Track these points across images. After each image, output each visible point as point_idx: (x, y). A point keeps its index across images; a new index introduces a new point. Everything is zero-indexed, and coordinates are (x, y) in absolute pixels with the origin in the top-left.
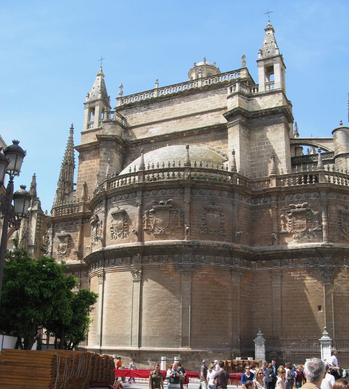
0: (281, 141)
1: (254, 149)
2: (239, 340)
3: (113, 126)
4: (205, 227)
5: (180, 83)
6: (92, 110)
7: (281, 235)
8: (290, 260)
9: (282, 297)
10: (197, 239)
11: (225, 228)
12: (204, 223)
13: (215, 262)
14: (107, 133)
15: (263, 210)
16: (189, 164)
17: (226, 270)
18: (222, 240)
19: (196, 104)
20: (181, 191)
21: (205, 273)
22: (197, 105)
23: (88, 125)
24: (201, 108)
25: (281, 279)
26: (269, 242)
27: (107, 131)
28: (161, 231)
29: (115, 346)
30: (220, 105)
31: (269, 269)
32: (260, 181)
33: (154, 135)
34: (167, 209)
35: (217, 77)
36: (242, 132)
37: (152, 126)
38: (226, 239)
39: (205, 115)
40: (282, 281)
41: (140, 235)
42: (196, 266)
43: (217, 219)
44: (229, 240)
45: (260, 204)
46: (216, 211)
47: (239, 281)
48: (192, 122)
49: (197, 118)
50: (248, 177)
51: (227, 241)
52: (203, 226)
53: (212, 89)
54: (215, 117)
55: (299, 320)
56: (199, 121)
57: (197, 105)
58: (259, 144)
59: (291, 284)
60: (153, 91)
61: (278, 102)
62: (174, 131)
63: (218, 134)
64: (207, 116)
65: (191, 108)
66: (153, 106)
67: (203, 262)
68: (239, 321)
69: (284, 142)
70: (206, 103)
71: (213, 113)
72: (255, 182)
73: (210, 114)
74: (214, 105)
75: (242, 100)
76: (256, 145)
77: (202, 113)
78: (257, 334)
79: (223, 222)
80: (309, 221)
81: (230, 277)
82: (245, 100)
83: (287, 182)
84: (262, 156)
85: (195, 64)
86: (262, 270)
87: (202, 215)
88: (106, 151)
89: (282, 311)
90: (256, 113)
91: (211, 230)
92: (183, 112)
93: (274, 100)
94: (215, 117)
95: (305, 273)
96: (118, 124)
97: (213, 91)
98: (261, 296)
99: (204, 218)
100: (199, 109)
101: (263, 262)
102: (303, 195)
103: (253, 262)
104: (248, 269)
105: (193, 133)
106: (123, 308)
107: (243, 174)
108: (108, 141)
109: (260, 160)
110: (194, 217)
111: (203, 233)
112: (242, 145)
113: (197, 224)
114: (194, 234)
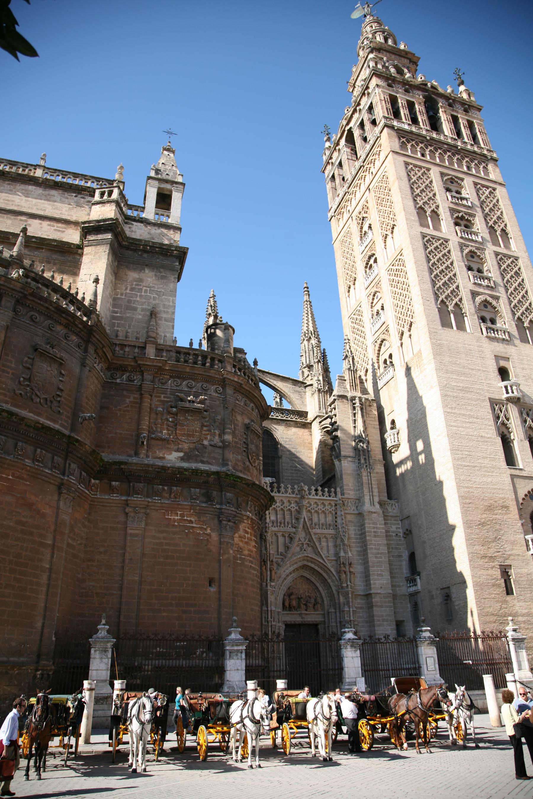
4: (28, 386)
7: (153, 442)
8: (166, 488)
9: (143, 555)
10: (7, 402)
12: (28, 377)
13: (34, 460)
15: (125, 393)
24: (32, 208)
30: (69, 215)
36: (110, 259)
40: (146, 524)
51: (62, 425)
52: (24, 382)
53: (59, 189)
54: (55, 230)
55: (173, 602)
58: (132, 289)
59: (162, 532)
63: (55, 256)
64: (41, 224)
65: (13, 201)
67: (9, 455)
80: (205, 428)
81: (56, 497)
84: (135, 309)
89: (141, 583)
90: (137, 243)
94: (55, 230)
95: (191, 515)
97: (61, 192)
98: (102, 550)
99: (30, 366)
101: (114, 483)
102: (199, 385)
105: (9, 239)
109: (129, 313)
110: (9, 358)
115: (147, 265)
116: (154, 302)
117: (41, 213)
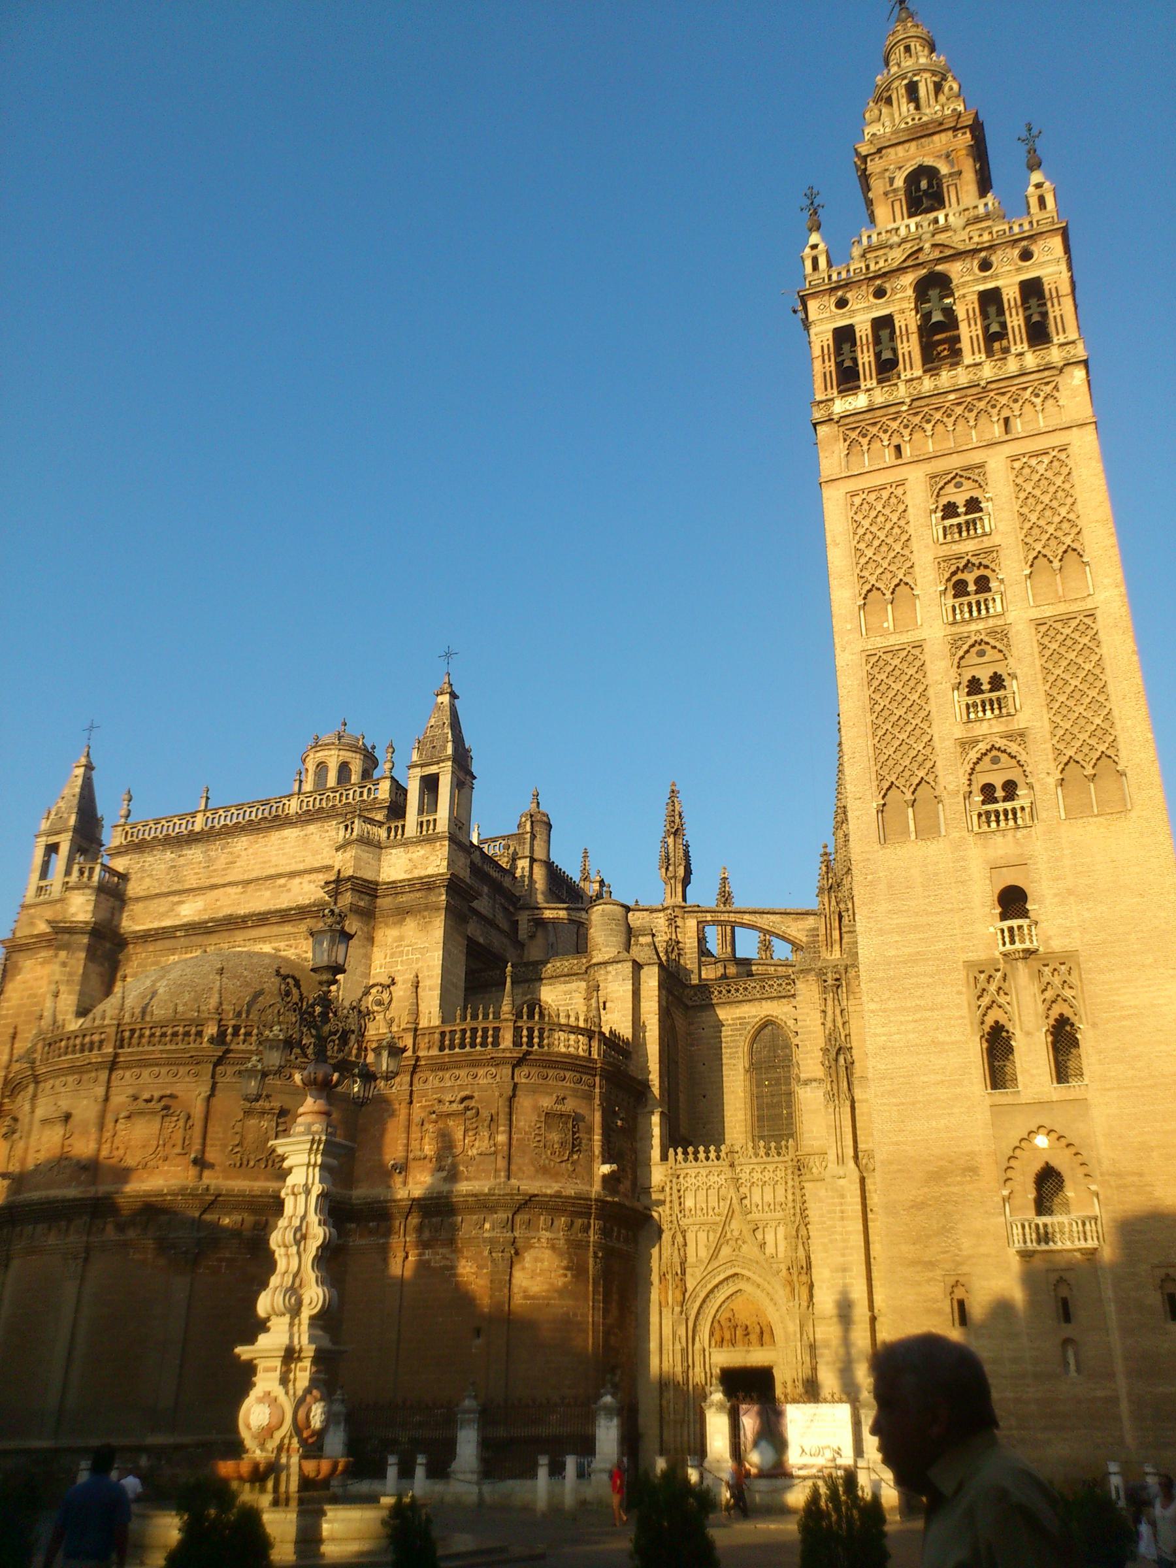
6: (52, 849)
19: (281, 852)
22: (283, 854)
23: (40, 889)
33: (185, 920)
39: (297, 880)
48: (268, 894)
49: (280, 886)
56: (282, 892)
57: (283, 854)
62: (229, 913)
65: (270, 861)
69: (441, 952)
71: (314, 876)
73: (307, 877)
77: (292, 875)
92: (253, 870)
93: (432, 858)
117: (301, 867)
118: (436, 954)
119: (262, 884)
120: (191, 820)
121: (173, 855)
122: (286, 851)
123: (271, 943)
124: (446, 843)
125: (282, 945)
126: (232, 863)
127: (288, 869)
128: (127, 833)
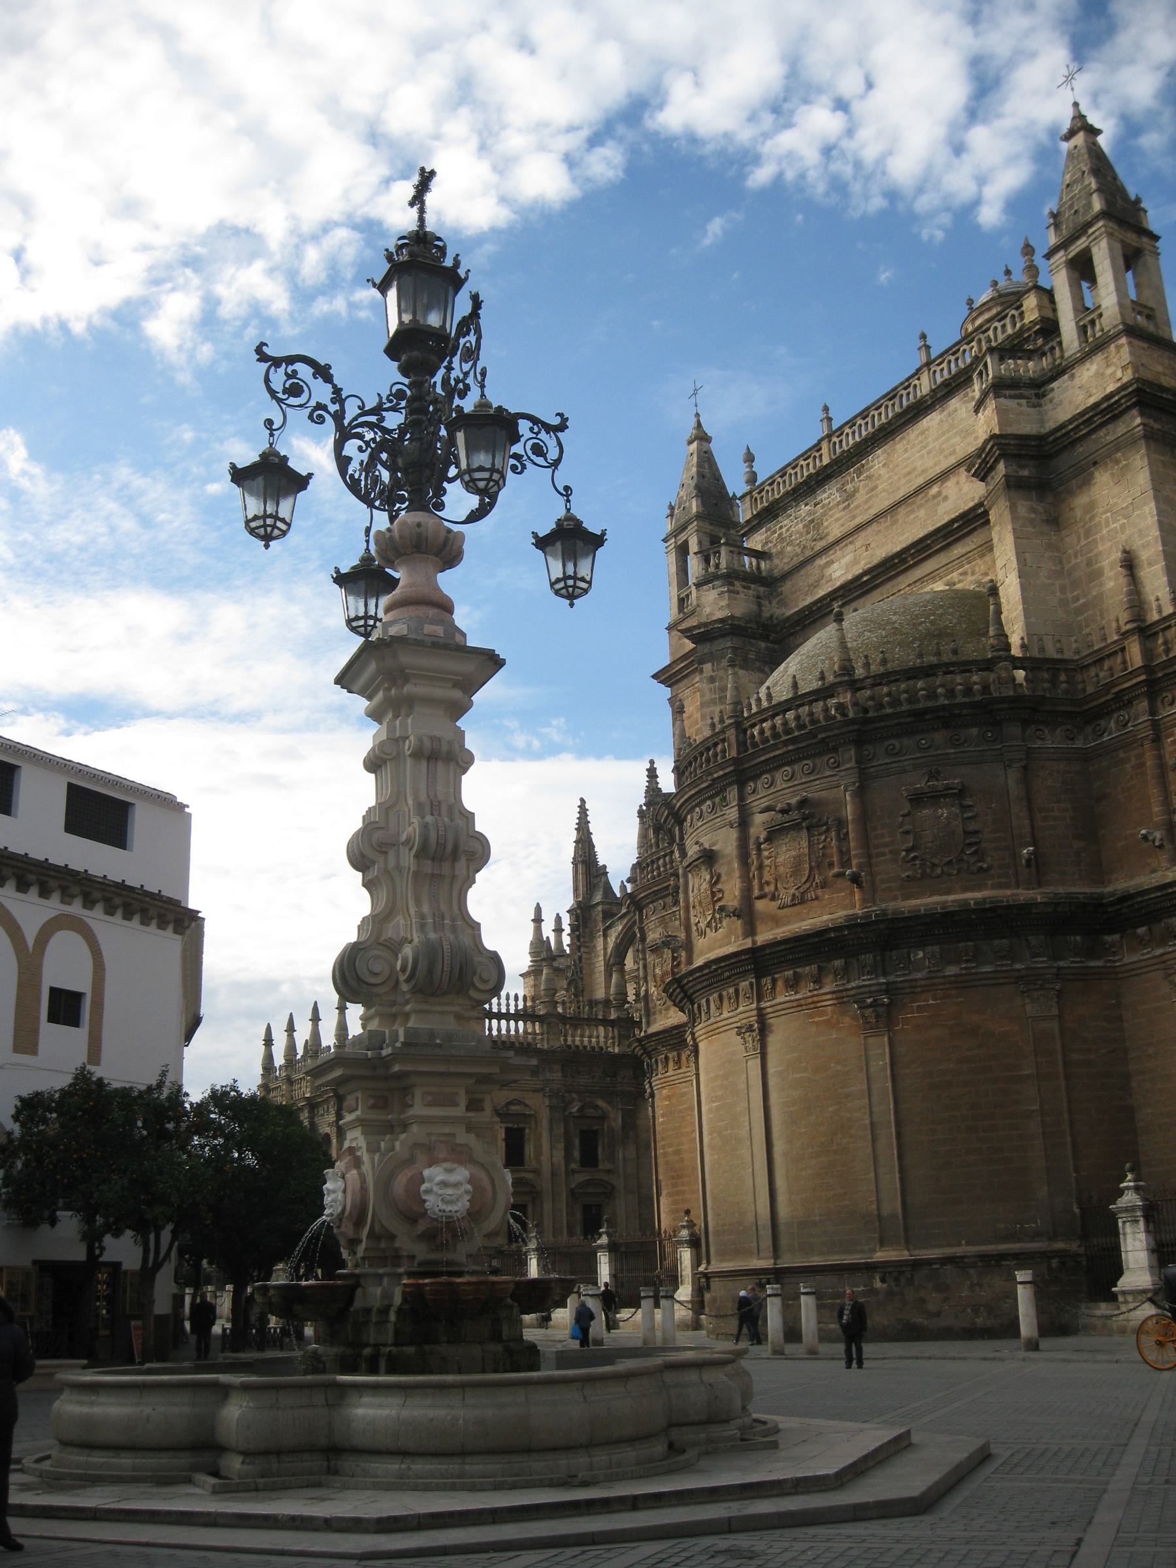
0: (1145, 504)
1: (1076, 557)
2: (1076, 1210)
3: (722, 589)
4: (915, 858)
5: (879, 400)
10: (895, 898)
11: (983, 845)
14: (711, 614)
16: (847, 668)
17: (1001, 981)
18: (979, 887)
19: (924, 451)
20: (832, 760)
21: (931, 1002)
22: (929, 453)
25: (1058, 1003)
26: (1149, 860)
27: (708, 610)
28: (794, 895)
29: (730, 1260)
31: (1159, 952)
32: (1102, 659)
33: (838, 584)
34: (797, 824)
35: (965, 347)
36: (1022, 510)
37: (831, 555)
38: (990, 882)
41: (747, 915)
42: (900, 985)
43: (949, 823)
44: (1004, 880)
45: (1109, 735)
46: (945, 796)
47: (1055, 1011)
48: (922, 513)
49: (934, 497)
50: (1068, 655)
51: (993, 887)
52: (907, 855)
56: (938, 504)
60: (817, 447)
61: (1119, 374)
64: (958, 483)
65: (915, 469)
66: (825, 495)
68: (1069, 1146)
69: (1153, 504)
70: (948, 439)
72: (1089, 665)
74: (970, 439)
75: (1011, 404)
76: (1079, 541)
78: (1122, 1185)
79: (972, 827)
82: (1024, 402)
83: (1162, 648)
85: (970, 302)
86: (1141, 961)
87: (900, 819)
88: (713, 671)
91: (936, 861)
92: (898, 489)
96: (737, 578)
99: (911, 827)
100: (935, 465)
103: (1108, 938)
104: (1092, 964)
106: (733, 1142)
107: (1042, 649)
108: (715, 638)
111: (908, 877)
112: (1027, 555)
113: (891, 852)
114: (884, 886)
115: (1095, 463)
116: (1124, 537)
118: (1147, 509)
119: (913, 503)
120: (817, 455)
121: (808, 507)
122: (931, 446)
123: (941, 578)
124: (1123, 340)
125: (955, 576)
126: (872, 490)
127: (938, 470)
128: (756, 499)
